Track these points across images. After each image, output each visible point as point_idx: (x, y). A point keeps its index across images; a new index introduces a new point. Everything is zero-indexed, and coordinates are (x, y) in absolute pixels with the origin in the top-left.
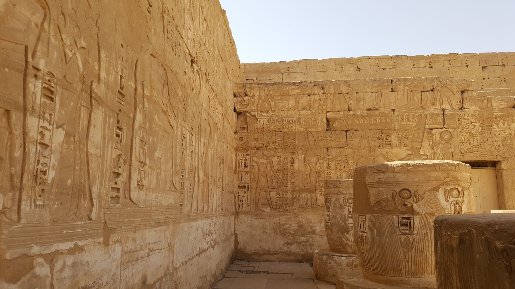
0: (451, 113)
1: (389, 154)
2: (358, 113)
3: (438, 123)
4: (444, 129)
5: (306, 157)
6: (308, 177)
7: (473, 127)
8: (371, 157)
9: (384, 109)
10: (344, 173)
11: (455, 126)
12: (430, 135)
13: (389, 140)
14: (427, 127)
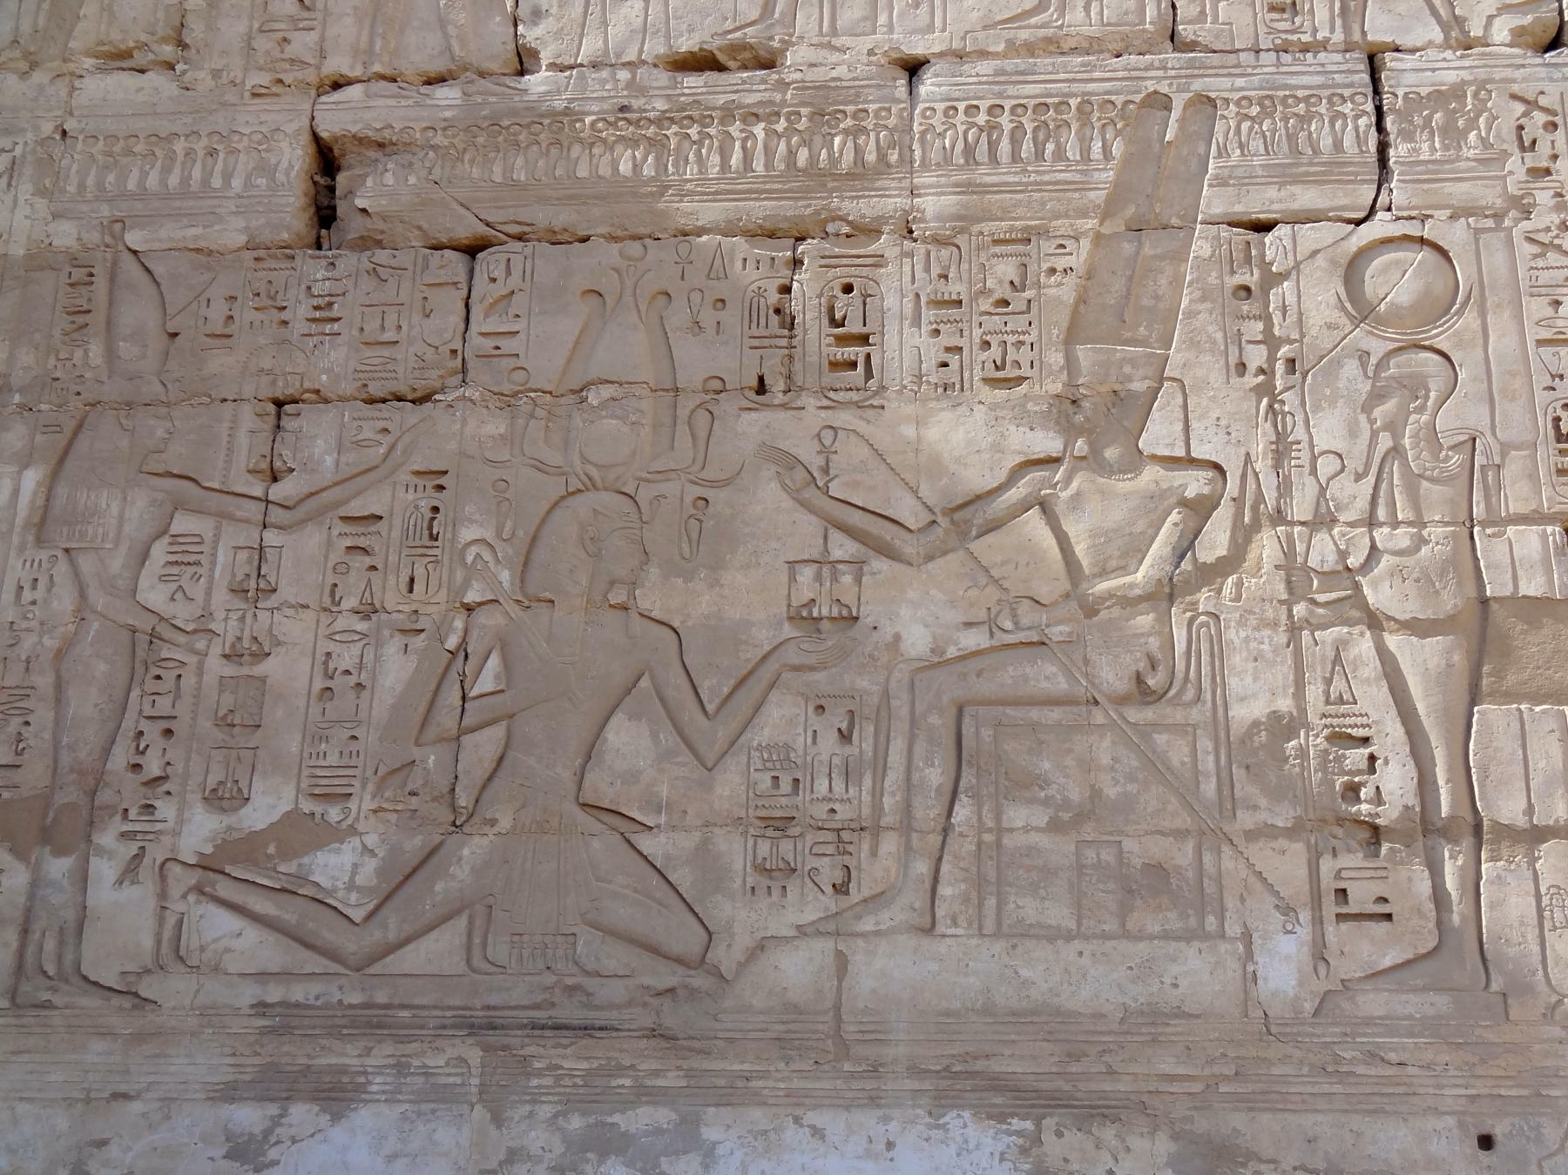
1: (850, 453)
4: (1381, 226)
5: (62, 491)
6: (43, 681)
8: (671, 488)
10: (393, 648)
11: (1491, 197)
12: (1252, 278)
13: (853, 327)
14: (1213, 201)
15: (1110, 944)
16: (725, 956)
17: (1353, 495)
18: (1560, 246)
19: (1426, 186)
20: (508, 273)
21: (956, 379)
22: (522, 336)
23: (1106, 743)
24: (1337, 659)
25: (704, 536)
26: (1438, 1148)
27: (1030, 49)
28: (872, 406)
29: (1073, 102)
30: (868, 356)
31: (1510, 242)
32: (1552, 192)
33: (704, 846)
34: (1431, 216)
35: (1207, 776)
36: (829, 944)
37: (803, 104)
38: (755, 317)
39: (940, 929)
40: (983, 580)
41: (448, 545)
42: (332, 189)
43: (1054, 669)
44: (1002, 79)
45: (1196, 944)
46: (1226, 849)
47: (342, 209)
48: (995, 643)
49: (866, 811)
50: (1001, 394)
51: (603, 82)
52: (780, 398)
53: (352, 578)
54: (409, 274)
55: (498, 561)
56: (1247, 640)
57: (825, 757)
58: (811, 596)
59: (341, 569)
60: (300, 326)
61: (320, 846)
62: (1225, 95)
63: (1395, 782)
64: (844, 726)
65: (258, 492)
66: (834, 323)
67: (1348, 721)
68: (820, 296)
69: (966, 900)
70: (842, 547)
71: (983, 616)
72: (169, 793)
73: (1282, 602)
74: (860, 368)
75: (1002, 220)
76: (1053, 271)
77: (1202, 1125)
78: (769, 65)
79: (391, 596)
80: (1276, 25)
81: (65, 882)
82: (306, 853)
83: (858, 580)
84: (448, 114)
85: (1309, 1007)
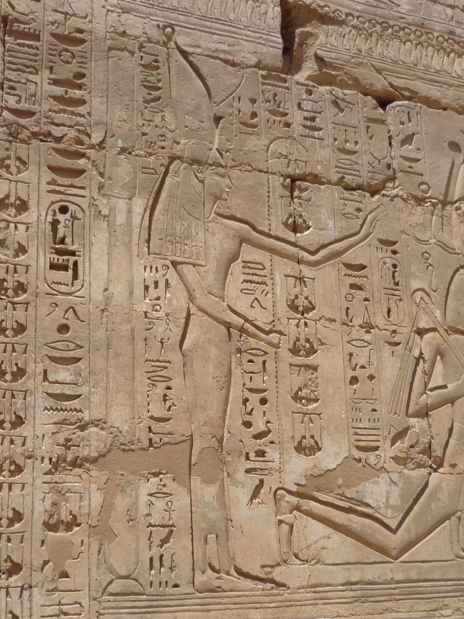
61: (367, 480)
72: (272, 442)
79: (379, 320)
81: (215, 503)
82: (358, 484)
84: (360, 7)
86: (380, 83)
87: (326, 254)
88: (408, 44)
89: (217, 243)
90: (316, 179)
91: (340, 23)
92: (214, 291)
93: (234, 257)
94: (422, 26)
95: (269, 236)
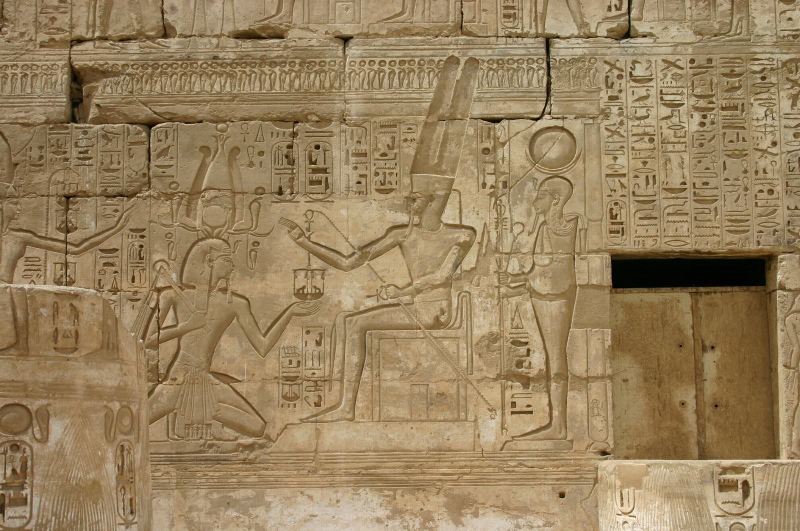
0: (579, 52)
1: (320, 221)
2: (201, 49)
3: (525, 96)
7: (665, 111)
8: (243, 237)
9: (303, 34)
10: (128, 306)
11: (593, 110)
12: (489, 144)
13: (321, 165)
14: (478, 110)
15: (425, 424)
16: (272, 431)
17: (527, 241)
18: (619, 132)
19: (566, 103)
20: (167, 138)
21: (364, 190)
22: (174, 167)
23: (424, 345)
24: (517, 310)
25: (256, 258)
26: (545, 498)
27: (398, 33)
28: (328, 201)
29: (417, 60)
30: (327, 179)
31: (599, 128)
32: (617, 108)
33: (262, 389)
34: (566, 118)
35: (463, 358)
36: (313, 426)
37: (297, 58)
38: (277, 160)
39: (357, 419)
40: (375, 277)
41: (148, 262)
42: (80, 90)
43: (404, 315)
44: (384, 48)
45: (457, 423)
46: (469, 386)
47: (85, 101)
48: (379, 304)
49: (327, 373)
50: (383, 196)
51: (205, 45)
52: (289, 197)
53: (107, 276)
54: (121, 137)
55: (170, 269)
56: (481, 303)
57: (310, 352)
58: (304, 284)
59: (102, 272)
60: (74, 161)
62: (483, 58)
63: (537, 360)
64: (318, 339)
65: (63, 238)
66: (311, 163)
67: (519, 336)
68: (305, 150)
69: (368, 408)
70: (317, 263)
71: (375, 293)
73: (496, 287)
74: (323, 184)
75: (385, 116)
76: (406, 140)
77: (457, 491)
78: (281, 37)
79: (125, 285)
80: (506, 24)
83: (323, 278)
84: (134, 57)
85: (499, 447)
86: (145, 113)
87: (88, 244)
88: (175, 76)
89: (8, 248)
90: (85, 194)
91: (117, 74)
92: (5, 278)
93: (21, 254)
94: (189, 58)
95: (46, 238)
